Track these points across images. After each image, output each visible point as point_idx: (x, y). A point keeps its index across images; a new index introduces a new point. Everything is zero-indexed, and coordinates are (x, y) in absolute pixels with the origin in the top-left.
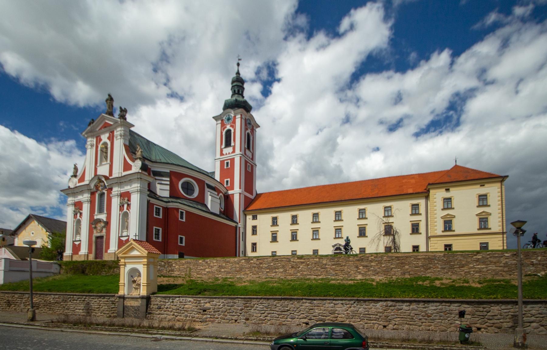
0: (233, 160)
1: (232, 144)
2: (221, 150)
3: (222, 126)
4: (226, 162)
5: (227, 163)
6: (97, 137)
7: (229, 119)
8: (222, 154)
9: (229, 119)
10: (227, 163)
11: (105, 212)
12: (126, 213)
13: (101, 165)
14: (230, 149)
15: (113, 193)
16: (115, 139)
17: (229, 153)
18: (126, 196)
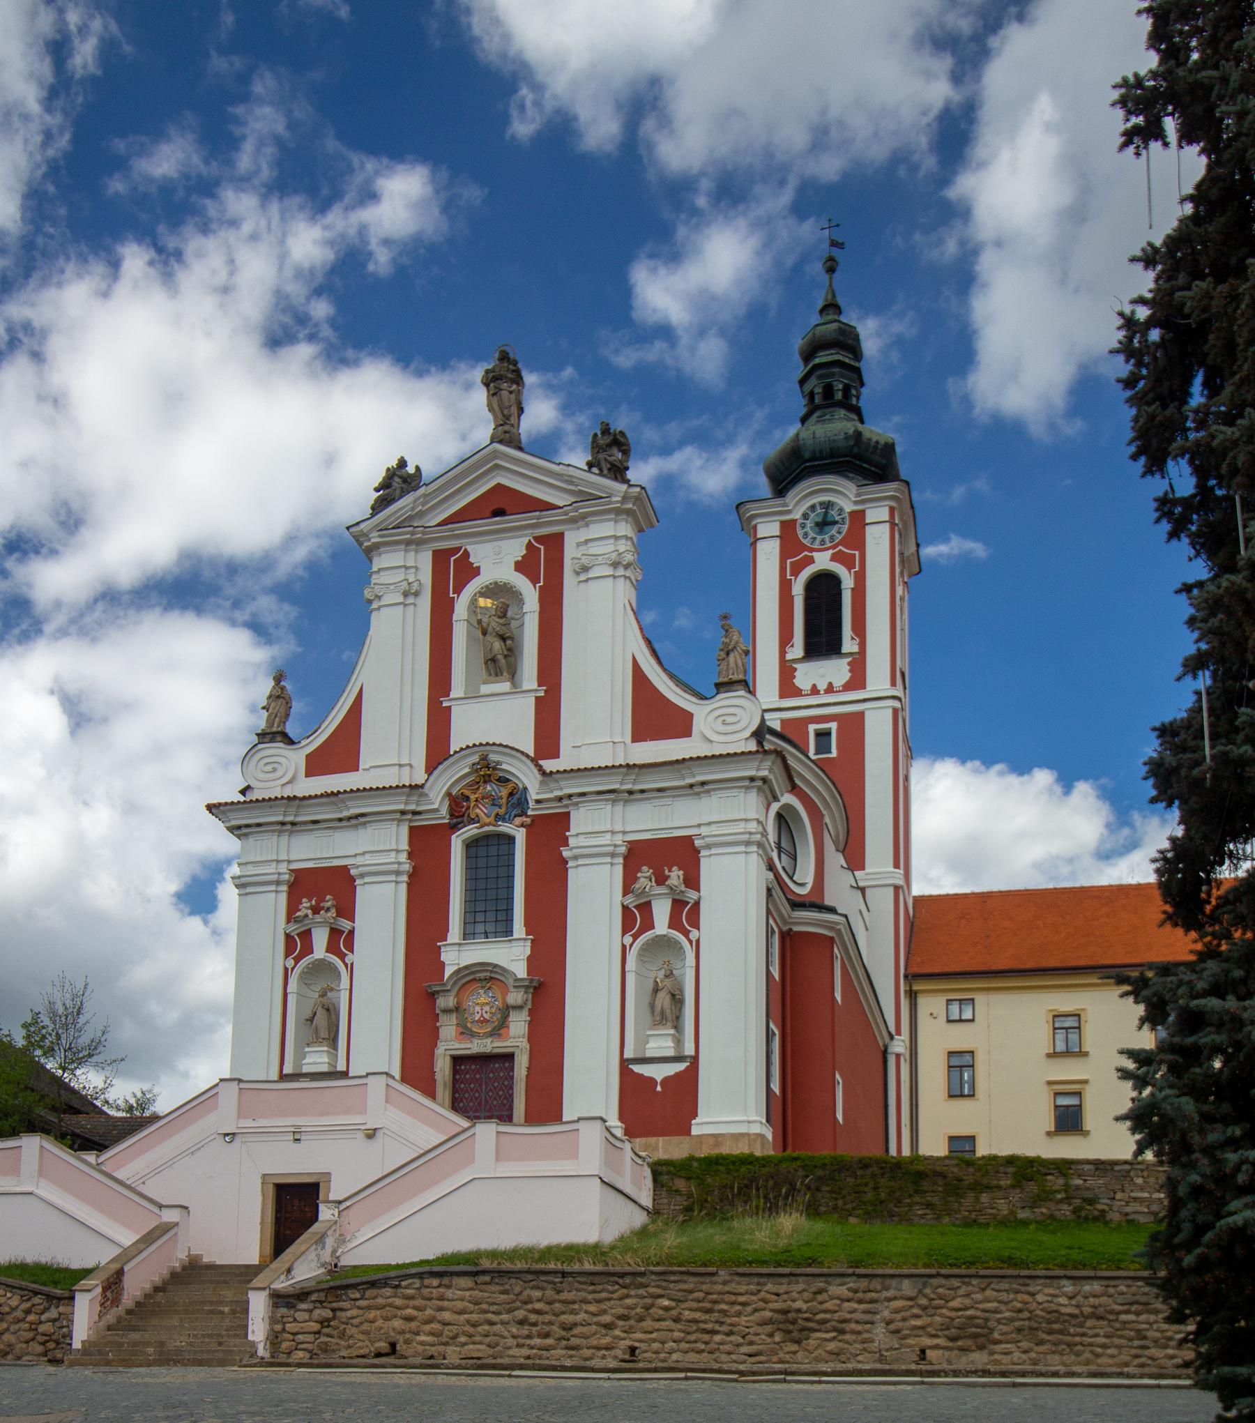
0: (853, 725)
1: (849, 644)
2: (787, 672)
3: (784, 557)
4: (812, 728)
5: (823, 735)
6: (440, 558)
7: (824, 524)
8: (788, 688)
9: (824, 524)
10: (823, 735)
11: (519, 928)
12: (662, 943)
13: (472, 696)
14: (835, 671)
15: (572, 842)
16: (569, 580)
17: (830, 689)
18: (666, 862)
